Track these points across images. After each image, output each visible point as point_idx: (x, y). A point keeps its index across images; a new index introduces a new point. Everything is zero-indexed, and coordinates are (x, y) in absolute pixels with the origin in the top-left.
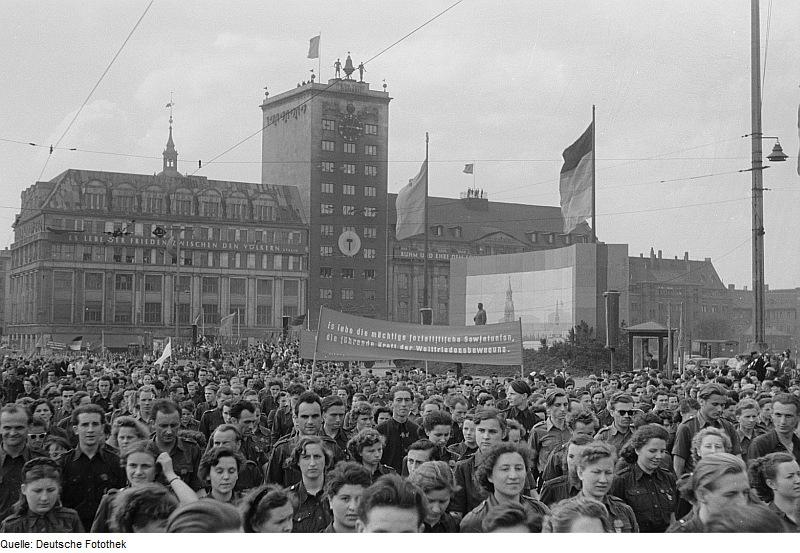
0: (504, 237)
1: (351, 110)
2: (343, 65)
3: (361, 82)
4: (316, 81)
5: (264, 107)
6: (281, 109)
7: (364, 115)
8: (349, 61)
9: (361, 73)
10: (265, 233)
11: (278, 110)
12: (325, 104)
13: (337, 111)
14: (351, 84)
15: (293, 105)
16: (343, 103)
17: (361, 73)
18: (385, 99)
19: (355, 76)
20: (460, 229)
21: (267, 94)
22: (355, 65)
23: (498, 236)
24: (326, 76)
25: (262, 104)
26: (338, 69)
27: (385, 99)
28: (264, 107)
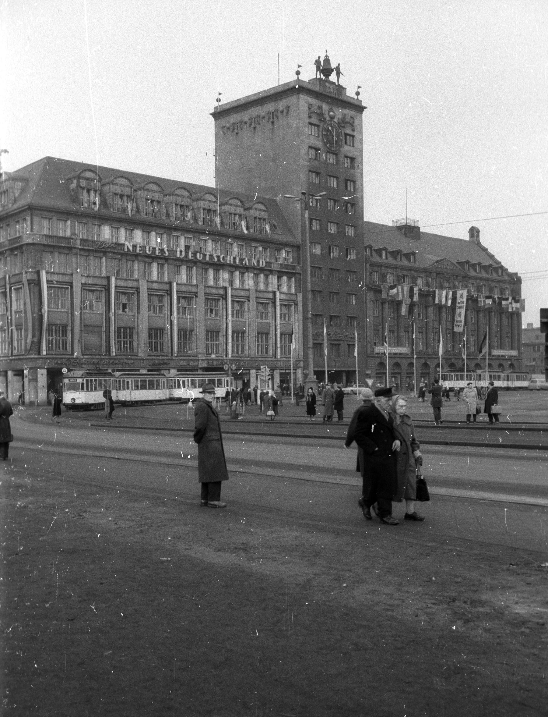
3: (339, 85)
4: (301, 77)
6: (246, 116)
7: (343, 123)
8: (327, 60)
11: (231, 117)
12: (310, 106)
13: (320, 115)
15: (270, 107)
16: (325, 107)
19: (333, 78)
21: (218, 100)
22: (333, 65)
24: (309, 74)
25: (212, 111)
26: (318, 69)
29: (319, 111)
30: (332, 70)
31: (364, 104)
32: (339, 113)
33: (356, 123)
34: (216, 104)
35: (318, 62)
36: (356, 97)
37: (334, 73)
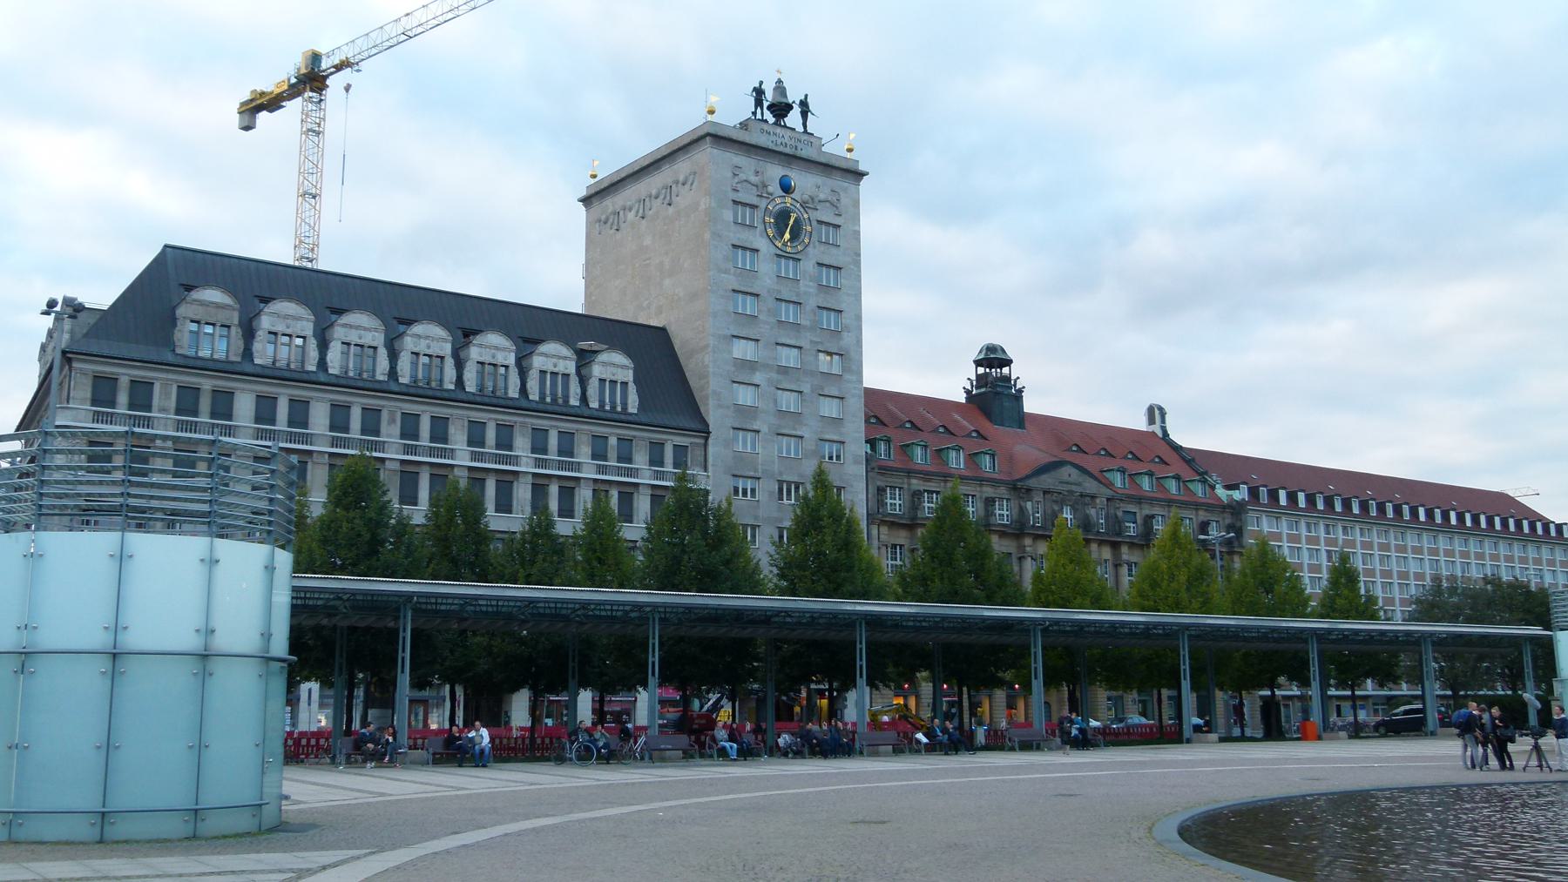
0: (1074, 472)
1: (786, 188)
2: (769, 96)
5: (586, 201)
9: (805, 114)
10: (613, 441)
14: (789, 133)
17: (805, 114)
18: (859, 175)
19: (794, 119)
20: (993, 456)
22: (794, 96)
23: (1067, 473)
24: (734, 111)
25: (584, 193)
26: (759, 103)
27: (859, 175)
28: (586, 201)
29: (753, 179)
30: (789, 107)
31: (862, 168)
32: (805, 183)
33: (845, 200)
34: (593, 181)
35: (759, 93)
36: (848, 155)
37: (796, 111)
